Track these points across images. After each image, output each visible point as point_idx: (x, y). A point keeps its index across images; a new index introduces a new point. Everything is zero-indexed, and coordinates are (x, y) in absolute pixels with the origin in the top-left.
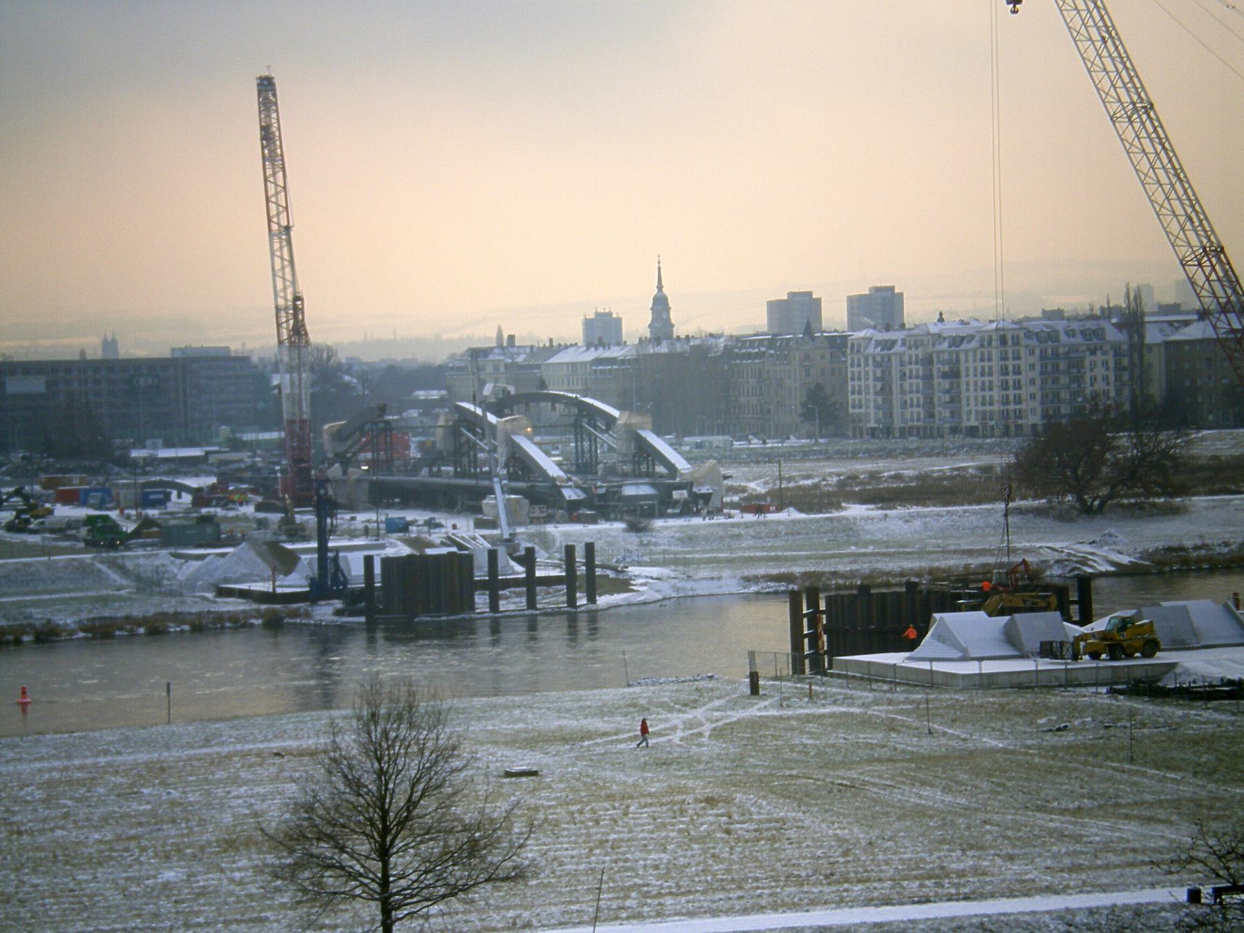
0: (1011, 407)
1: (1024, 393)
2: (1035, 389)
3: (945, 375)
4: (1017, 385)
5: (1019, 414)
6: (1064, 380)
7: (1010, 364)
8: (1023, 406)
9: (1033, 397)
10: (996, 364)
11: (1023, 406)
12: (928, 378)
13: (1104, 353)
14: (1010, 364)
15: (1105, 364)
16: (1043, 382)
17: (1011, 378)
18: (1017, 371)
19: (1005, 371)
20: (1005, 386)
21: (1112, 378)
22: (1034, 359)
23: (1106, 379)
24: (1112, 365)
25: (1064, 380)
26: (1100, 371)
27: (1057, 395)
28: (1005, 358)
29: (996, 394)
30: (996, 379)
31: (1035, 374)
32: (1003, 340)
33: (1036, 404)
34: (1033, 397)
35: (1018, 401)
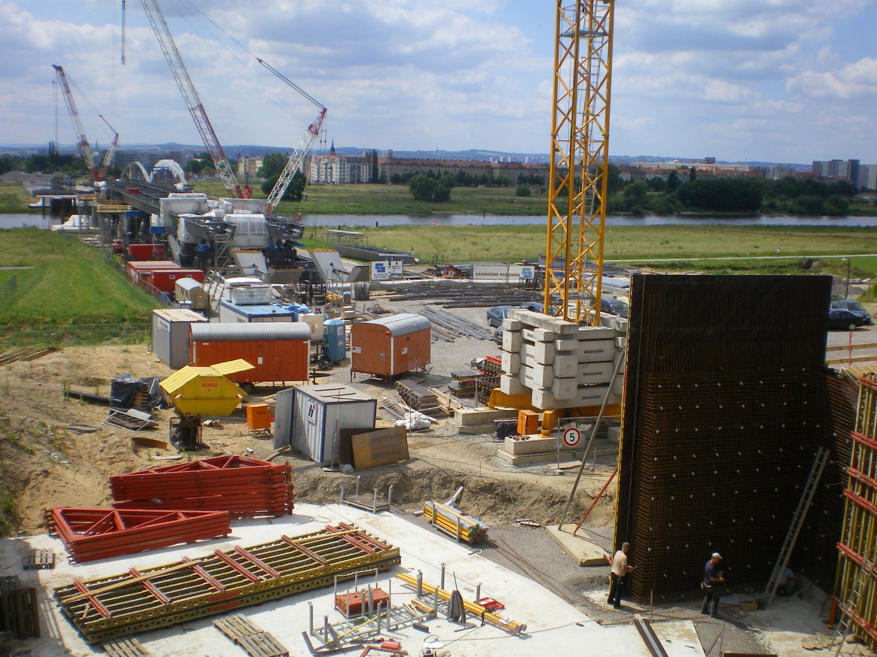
1: (346, 174)
2: (349, 173)
4: (344, 172)
5: (344, 179)
10: (338, 166)
12: (326, 168)
18: (344, 168)
19: (341, 168)
20: (341, 172)
26: (365, 170)
28: (341, 164)
29: (338, 174)
30: (338, 170)
31: (349, 169)
32: (341, 160)
33: (349, 177)
35: (344, 175)
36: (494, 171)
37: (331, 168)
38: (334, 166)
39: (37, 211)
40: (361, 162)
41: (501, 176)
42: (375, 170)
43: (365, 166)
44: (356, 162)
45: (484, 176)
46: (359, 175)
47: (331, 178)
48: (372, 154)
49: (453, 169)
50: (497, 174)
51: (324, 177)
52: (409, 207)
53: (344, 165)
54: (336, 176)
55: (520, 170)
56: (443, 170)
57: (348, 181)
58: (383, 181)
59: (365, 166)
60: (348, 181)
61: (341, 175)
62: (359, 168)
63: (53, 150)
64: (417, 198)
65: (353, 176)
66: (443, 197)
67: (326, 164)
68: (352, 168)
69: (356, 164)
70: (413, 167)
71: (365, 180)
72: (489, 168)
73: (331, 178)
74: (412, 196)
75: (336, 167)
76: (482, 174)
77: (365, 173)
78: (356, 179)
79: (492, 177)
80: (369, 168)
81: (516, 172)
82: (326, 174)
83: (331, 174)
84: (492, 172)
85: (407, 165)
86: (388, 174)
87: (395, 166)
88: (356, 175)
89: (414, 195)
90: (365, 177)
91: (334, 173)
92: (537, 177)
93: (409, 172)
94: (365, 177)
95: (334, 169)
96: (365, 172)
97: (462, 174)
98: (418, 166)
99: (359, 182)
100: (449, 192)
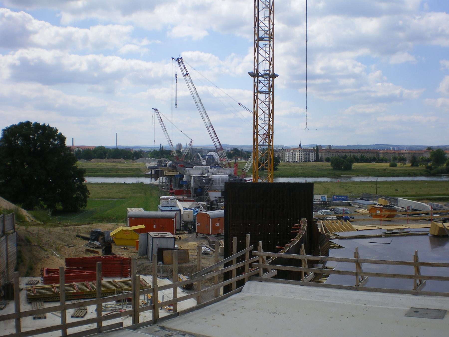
0: (301, 159)
1: (302, 157)
2: (304, 157)
3: (294, 155)
4: (301, 156)
5: (301, 160)
6: (307, 156)
7: (301, 154)
8: (302, 159)
9: (303, 158)
10: (299, 154)
11: (302, 159)
12: (292, 155)
13: (313, 153)
14: (301, 154)
15: (313, 154)
16: (305, 156)
17: (301, 155)
18: (301, 155)
19: (300, 154)
20: (300, 156)
21: (313, 156)
22: (304, 153)
23: (313, 156)
24: (313, 154)
25: (307, 156)
26: (312, 155)
27: (306, 158)
28: (300, 153)
29: (299, 157)
30: (299, 155)
31: (304, 155)
32: (300, 151)
33: (304, 159)
34: (303, 158)
36: (380, 154)
37: (295, 155)
38: (296, 154)
39: (149, 176)
40: (309, 151)
41: (383, 157)
42: (317, 156)
43: (312, 153)
44: (307, 151)
45: (374, 157)
46: (309, 158)
47: (295, 159)
48: (316, 147)
49: (358, 154)
50: (381, 156)
51: (291, 159)
52: (329, 173)
53: (301, 153)
54: (297, 159)
55: (394, 154)
56: (352, 154)
57: (304, 161)
58: (321, 161)
59: (312, 153)
60: (304, 161)
61: (300, 158)
62: (309, 154)
63: (162, 148)
64: (334, 169)
65: (306, 158)
66: (348, 168)
67: (293, 153)
68: (306, 155)
69: (307, 152)
70: (337, 153)
71: (312, 160)
72: (377, 153)
73: (295, 159)
74: (332, 168)
75: (297, 154)
76: (373, 157)
77: (312, 157)
78: (307, 160)
79: (378, 158)
80: (314, 154)
81: (392, 155)
82: (293, 158)
83: (295, 158)
84: (379, 155)
85: (334, 152)
86: (324, 157)
87: (328, 153)
88: (307, 158)
89: (333, 167)
90: (312, 159)
91: (296, 157)
92: (403, 157)
93: (335, 155)
94: (312, 159)
95: (296, 155)
96: (312, 156)
97: (362, 156)
98: (340, 153)
99: (309, 161)
100: (351, 165)
